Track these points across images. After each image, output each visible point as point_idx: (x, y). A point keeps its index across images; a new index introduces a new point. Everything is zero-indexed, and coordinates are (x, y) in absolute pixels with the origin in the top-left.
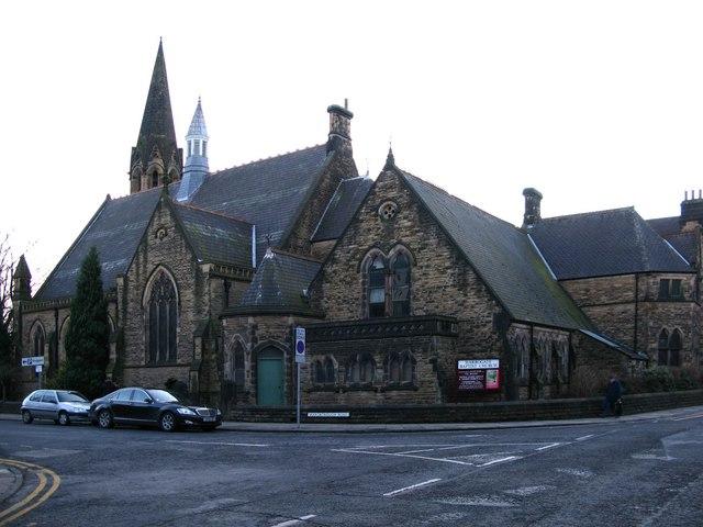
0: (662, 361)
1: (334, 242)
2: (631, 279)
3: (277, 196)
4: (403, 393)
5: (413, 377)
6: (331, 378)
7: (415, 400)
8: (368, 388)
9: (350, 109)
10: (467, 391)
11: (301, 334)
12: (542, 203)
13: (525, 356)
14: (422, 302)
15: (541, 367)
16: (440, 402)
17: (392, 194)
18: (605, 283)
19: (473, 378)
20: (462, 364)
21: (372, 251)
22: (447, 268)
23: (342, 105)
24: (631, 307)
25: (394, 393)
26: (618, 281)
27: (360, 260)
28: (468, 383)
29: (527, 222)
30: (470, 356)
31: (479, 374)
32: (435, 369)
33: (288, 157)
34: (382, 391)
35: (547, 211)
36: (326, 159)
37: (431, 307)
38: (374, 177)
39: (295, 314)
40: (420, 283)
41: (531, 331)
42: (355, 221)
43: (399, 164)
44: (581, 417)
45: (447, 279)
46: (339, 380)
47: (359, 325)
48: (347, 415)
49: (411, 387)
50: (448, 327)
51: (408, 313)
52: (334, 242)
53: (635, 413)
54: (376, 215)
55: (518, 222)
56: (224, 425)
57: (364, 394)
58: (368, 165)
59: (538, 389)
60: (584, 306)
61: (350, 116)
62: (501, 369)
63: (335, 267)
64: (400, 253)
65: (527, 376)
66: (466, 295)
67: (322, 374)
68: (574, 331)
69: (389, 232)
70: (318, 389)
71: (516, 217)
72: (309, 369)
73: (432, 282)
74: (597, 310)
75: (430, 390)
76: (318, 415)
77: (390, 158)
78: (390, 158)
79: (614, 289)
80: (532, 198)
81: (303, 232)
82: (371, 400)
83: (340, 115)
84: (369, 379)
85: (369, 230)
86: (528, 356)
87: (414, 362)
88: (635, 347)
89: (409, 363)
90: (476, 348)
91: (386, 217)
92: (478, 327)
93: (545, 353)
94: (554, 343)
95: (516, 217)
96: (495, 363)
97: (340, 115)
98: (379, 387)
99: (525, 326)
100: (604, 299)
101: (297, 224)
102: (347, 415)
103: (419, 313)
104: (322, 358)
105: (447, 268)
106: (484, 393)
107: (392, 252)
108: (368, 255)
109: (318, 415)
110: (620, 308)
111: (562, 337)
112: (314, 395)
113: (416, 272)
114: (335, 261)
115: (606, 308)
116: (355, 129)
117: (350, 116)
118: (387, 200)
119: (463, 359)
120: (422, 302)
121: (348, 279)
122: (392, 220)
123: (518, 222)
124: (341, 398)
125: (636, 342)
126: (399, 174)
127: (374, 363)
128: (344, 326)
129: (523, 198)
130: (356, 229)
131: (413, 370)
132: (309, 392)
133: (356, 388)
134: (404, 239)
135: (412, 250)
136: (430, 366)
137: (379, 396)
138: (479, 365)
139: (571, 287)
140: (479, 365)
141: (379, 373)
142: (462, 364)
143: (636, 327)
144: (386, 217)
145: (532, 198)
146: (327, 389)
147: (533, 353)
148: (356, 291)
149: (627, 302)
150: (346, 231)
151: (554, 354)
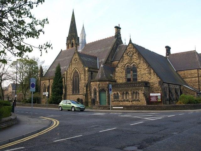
0: (45, 104)
1: (118, 62)
2: (196, 71)
3: (103, 50)
4: (137, 102)
5: (139, 98)
6: (119, 98)
7: (139, 103)
8: (127, 101)
9: (120, 27)
10: (153, 102)
11: (110, 86)
12: (171, 50)
13: (168, 92)
14: (140, 78)
15: (172, 95)
16: (146, 105)
17: (131, 50)
18: (189, 72)
19: (154, 98)
20: (151, 94)
21: (127, 64)
22: (146, 69)
23: (118, 26)
24: (197, 78)
25: (134, 102)
26: (193, 71)
27: (124, 67)
28: (153, 99)
29: (167, 55)
30: (153, 92)
31: (155, 97)
32: (144, 96)
33: (105, 39)
34: (131, 101)
35: (172, 52)
36: (115, 40)
37: (142, 79)
38: (127, 44)
39: (109, 81)
40: (139, 73)
41: (169, 85)
42: (122, 57)
43: (133, 42)
44: (184, 109)
45: (146, 72)
46: (120, 98)
47: (125, 84)
48: (123, 108)
49: (138, 100)
50: (147, 84)
51: (137, 80)
52: (118, 62)
53: (199, 109)
54: (128, 55)
55: (164, 55)
56: (86, 110)
57: (127, 102)
58: (125, 41)
59: (172, 101)
60: (184, 78)
61: (120, 29)
62: (161, 96)
63: (118, 69)
64: (134, 65)
65: (169, 98)
66: (151, 76)
67: (116, 97)
68: (181, 85)
69: (131, 59)
70: (115, 101)
71: (163, 53)
72: (113, 96)
73: (142, 73)
74: (188, 79)
75: (143, 101)
76: (115, 108)
77: (130, 41)
78: (130, 41)
79: (192, 73)
80: (168, 49)
81: (110, 59)
82: (129, 104)
83: (118, 28)
84: (128, 98)
85: (126, 59)
86: (168, 92)
87: (139, 94)
88: (199, 90)
89: (138, 94)
90: (154, 90)
91: (130, 55)
92: (155, 84)
93: (173, 92)
94: (176, 89)
95: (163, 53)
96: (159, 94)
97: (118, 28)
98: (130, 100)
99: (167, 84)
100: (189, 76)
101: (108, 57)
102: (123, 108)
103: (140, 81)
104: (116, 93)
105: (146, 69)
106: (157, 103)
107: (132, 65)
108: (126, 65)
109: (115, 108)
110: (194, 79)
111: (178, 87)
112: (114, 102)
113: (138, 70)
114: (118, 67)
115: (190, 79)
116: (122, 32)
117: (120, 29)
118: (130, 51)
119: (151, 93)
120: (140, 78)
121: (121, 72)
122: (132, 56)
123: (164, 55)
124: (121, 104)
125: (199, 88)
126: (133, 44)
127: (129, 94)
128: (121, 84)
129: (165, 49)
130: (123, 58)
131: (139, 96)
132: (113, 102)
133: (124, 101)
134: (135, 61)
135: (137, 64)
136: (143, 95)
137: (130, 103)
138: (155, 95)
139: (180, 73)
140: (155, 95)
141: (130, 97)
142: (151, 94)
143: (199, 84)
144: (130, 55)
145: (168, 49)
146: (117, 101)
147: (170, 91)
148: (124, 75)
149: (196, 77)
150: (120, 59)
151: (176, 92)
